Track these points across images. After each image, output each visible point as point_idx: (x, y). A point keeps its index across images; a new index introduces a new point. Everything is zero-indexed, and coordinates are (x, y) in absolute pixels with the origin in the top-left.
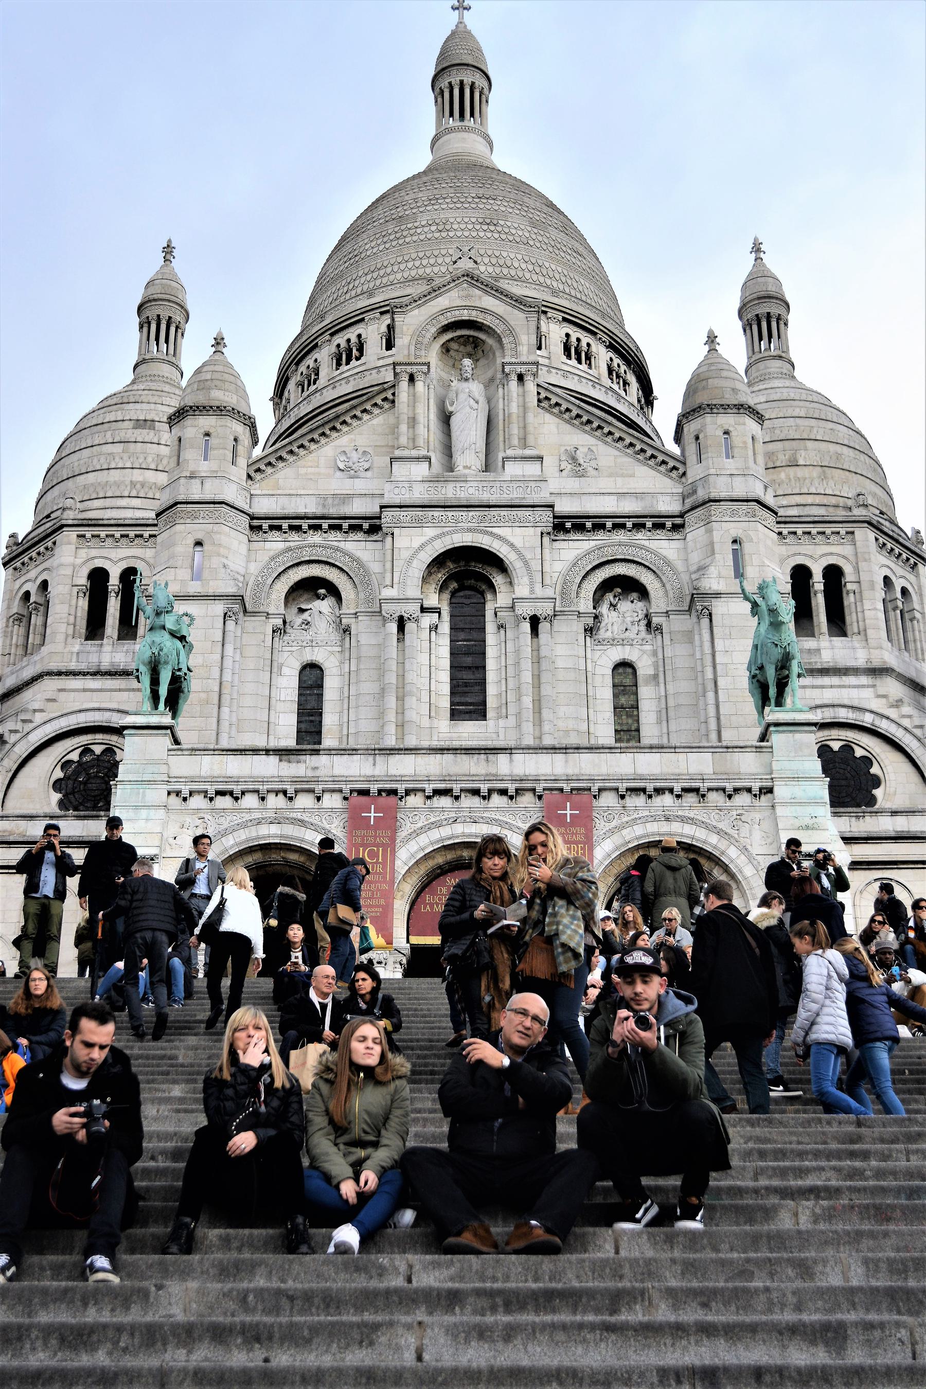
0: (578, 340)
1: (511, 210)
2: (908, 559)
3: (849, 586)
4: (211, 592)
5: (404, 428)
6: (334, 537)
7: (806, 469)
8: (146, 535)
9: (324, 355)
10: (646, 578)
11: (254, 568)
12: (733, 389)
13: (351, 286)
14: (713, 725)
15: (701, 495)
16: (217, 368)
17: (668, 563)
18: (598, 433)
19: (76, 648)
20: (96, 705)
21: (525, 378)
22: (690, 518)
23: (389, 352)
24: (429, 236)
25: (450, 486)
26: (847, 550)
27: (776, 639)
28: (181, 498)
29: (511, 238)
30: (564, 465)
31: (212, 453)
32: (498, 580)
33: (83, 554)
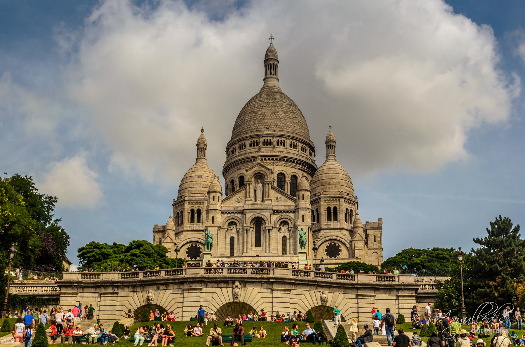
0: (294, 143)
1: (279, 109)
2: (353, 203)
3: (338, 211)
4: (215, 225)
5: (248, 194)
6: (236, 214)
7: (332, 186)
8: (201, 202)
9: (237, 146)
10: (289, 221)
11: (222, 220)
12: (305, 186)
14: (297, 248)
16: (215, 183)
17: (292, 219)
19: (189, 225)
20: (193, 237)
23: (251, 148)
24: (260, 118)
25: (255, 205)
26: (338, 203)
28: (210, 209)
29: (279, 117)
30: (276, 200)
31: (215, 200)
32: (263, 222)
33: (189, 206)
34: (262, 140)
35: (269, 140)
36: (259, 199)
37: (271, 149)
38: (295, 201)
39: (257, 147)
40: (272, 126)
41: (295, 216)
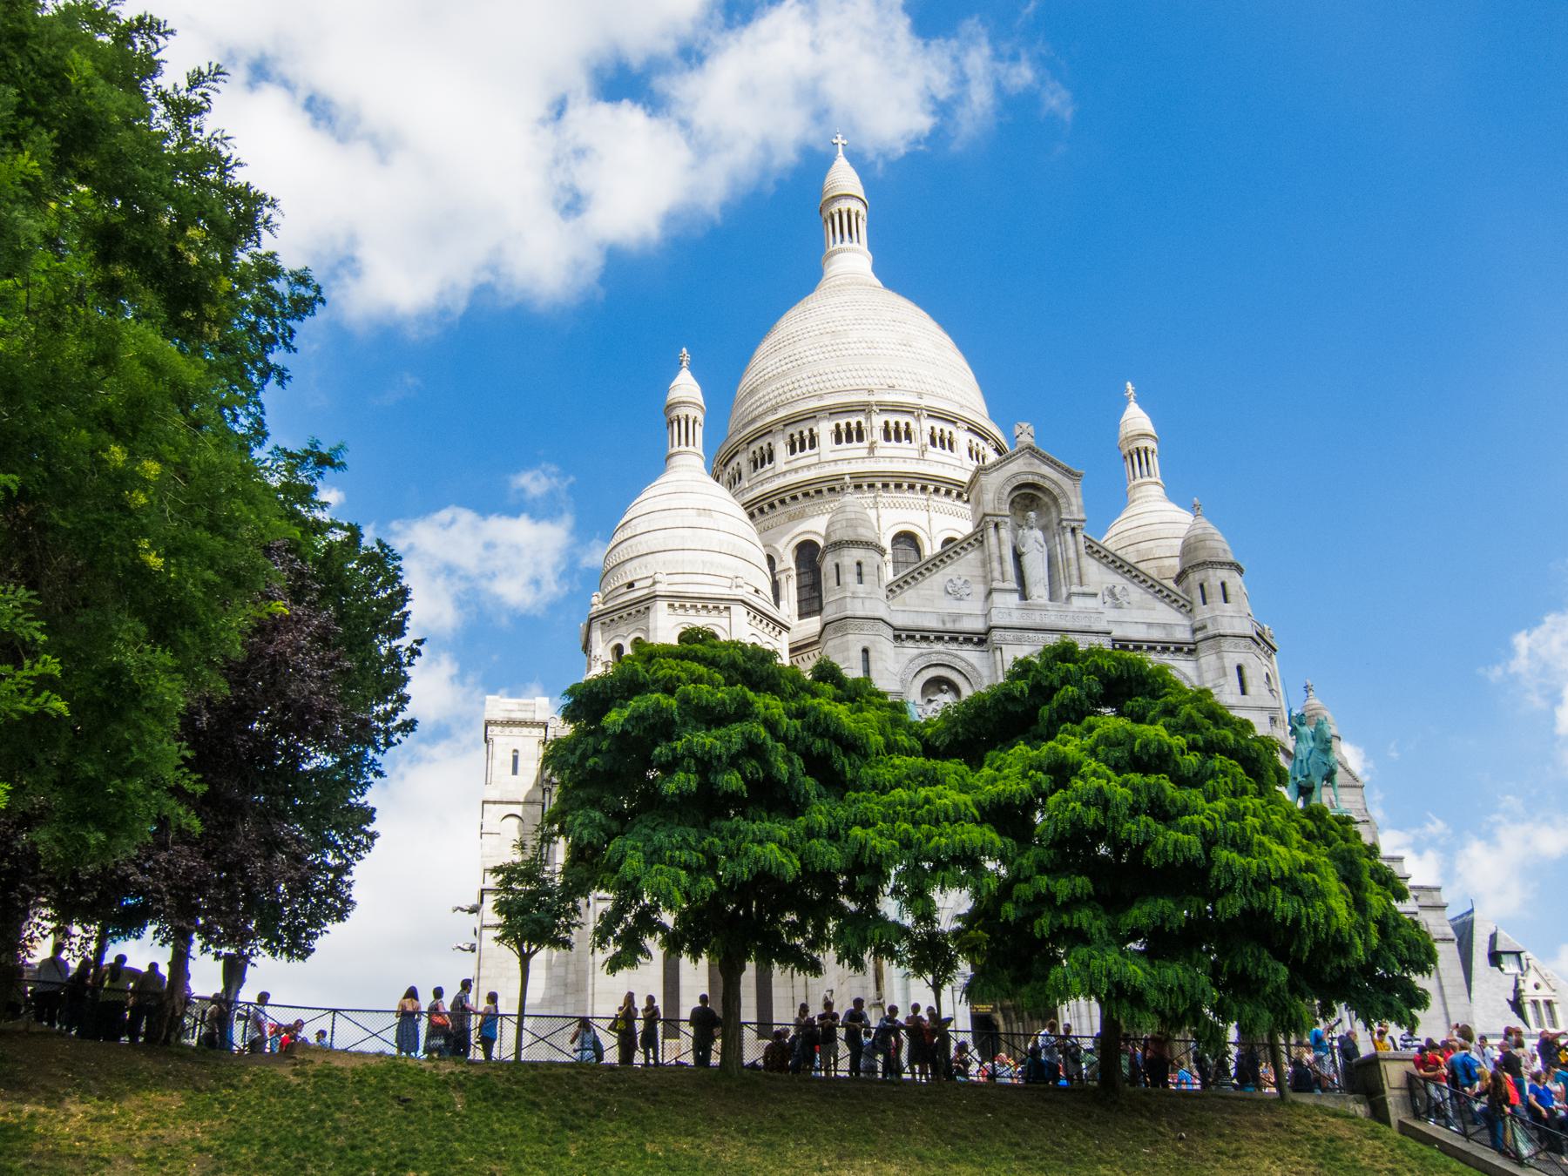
5: (996, 565)
6: (953, 647)
8: (722, 607)
13: (796, 385)
15: (1211, 631)
18: (1128, 575)
21: (1078, 531)
22: (1200, 645)
23: (839, 447)
25: (1037, 613)
27: (1325, 760)
28: (849, 613)
30: (1107, 599)
31: (865, 578)
34: (878, 421)
35: (903, 427)
36: (1039, 591)
37: (916, 454)
38: (1186, 608)
39: (860, 445)
40: (906, 383)
41: (1198, 668)
